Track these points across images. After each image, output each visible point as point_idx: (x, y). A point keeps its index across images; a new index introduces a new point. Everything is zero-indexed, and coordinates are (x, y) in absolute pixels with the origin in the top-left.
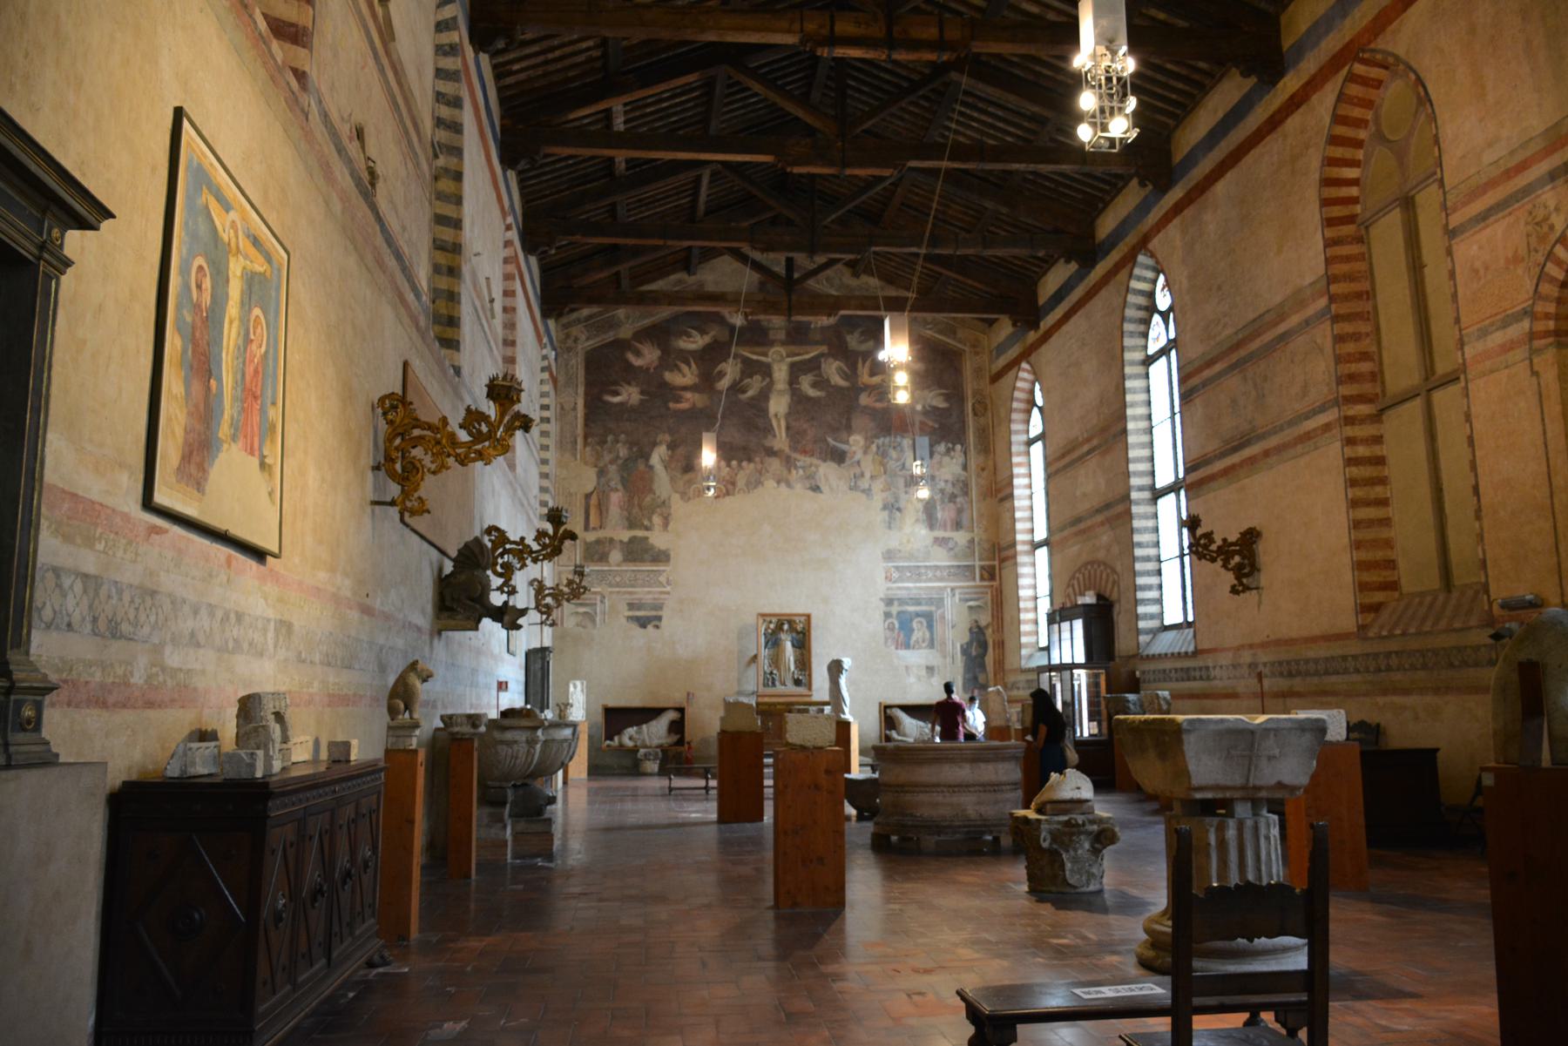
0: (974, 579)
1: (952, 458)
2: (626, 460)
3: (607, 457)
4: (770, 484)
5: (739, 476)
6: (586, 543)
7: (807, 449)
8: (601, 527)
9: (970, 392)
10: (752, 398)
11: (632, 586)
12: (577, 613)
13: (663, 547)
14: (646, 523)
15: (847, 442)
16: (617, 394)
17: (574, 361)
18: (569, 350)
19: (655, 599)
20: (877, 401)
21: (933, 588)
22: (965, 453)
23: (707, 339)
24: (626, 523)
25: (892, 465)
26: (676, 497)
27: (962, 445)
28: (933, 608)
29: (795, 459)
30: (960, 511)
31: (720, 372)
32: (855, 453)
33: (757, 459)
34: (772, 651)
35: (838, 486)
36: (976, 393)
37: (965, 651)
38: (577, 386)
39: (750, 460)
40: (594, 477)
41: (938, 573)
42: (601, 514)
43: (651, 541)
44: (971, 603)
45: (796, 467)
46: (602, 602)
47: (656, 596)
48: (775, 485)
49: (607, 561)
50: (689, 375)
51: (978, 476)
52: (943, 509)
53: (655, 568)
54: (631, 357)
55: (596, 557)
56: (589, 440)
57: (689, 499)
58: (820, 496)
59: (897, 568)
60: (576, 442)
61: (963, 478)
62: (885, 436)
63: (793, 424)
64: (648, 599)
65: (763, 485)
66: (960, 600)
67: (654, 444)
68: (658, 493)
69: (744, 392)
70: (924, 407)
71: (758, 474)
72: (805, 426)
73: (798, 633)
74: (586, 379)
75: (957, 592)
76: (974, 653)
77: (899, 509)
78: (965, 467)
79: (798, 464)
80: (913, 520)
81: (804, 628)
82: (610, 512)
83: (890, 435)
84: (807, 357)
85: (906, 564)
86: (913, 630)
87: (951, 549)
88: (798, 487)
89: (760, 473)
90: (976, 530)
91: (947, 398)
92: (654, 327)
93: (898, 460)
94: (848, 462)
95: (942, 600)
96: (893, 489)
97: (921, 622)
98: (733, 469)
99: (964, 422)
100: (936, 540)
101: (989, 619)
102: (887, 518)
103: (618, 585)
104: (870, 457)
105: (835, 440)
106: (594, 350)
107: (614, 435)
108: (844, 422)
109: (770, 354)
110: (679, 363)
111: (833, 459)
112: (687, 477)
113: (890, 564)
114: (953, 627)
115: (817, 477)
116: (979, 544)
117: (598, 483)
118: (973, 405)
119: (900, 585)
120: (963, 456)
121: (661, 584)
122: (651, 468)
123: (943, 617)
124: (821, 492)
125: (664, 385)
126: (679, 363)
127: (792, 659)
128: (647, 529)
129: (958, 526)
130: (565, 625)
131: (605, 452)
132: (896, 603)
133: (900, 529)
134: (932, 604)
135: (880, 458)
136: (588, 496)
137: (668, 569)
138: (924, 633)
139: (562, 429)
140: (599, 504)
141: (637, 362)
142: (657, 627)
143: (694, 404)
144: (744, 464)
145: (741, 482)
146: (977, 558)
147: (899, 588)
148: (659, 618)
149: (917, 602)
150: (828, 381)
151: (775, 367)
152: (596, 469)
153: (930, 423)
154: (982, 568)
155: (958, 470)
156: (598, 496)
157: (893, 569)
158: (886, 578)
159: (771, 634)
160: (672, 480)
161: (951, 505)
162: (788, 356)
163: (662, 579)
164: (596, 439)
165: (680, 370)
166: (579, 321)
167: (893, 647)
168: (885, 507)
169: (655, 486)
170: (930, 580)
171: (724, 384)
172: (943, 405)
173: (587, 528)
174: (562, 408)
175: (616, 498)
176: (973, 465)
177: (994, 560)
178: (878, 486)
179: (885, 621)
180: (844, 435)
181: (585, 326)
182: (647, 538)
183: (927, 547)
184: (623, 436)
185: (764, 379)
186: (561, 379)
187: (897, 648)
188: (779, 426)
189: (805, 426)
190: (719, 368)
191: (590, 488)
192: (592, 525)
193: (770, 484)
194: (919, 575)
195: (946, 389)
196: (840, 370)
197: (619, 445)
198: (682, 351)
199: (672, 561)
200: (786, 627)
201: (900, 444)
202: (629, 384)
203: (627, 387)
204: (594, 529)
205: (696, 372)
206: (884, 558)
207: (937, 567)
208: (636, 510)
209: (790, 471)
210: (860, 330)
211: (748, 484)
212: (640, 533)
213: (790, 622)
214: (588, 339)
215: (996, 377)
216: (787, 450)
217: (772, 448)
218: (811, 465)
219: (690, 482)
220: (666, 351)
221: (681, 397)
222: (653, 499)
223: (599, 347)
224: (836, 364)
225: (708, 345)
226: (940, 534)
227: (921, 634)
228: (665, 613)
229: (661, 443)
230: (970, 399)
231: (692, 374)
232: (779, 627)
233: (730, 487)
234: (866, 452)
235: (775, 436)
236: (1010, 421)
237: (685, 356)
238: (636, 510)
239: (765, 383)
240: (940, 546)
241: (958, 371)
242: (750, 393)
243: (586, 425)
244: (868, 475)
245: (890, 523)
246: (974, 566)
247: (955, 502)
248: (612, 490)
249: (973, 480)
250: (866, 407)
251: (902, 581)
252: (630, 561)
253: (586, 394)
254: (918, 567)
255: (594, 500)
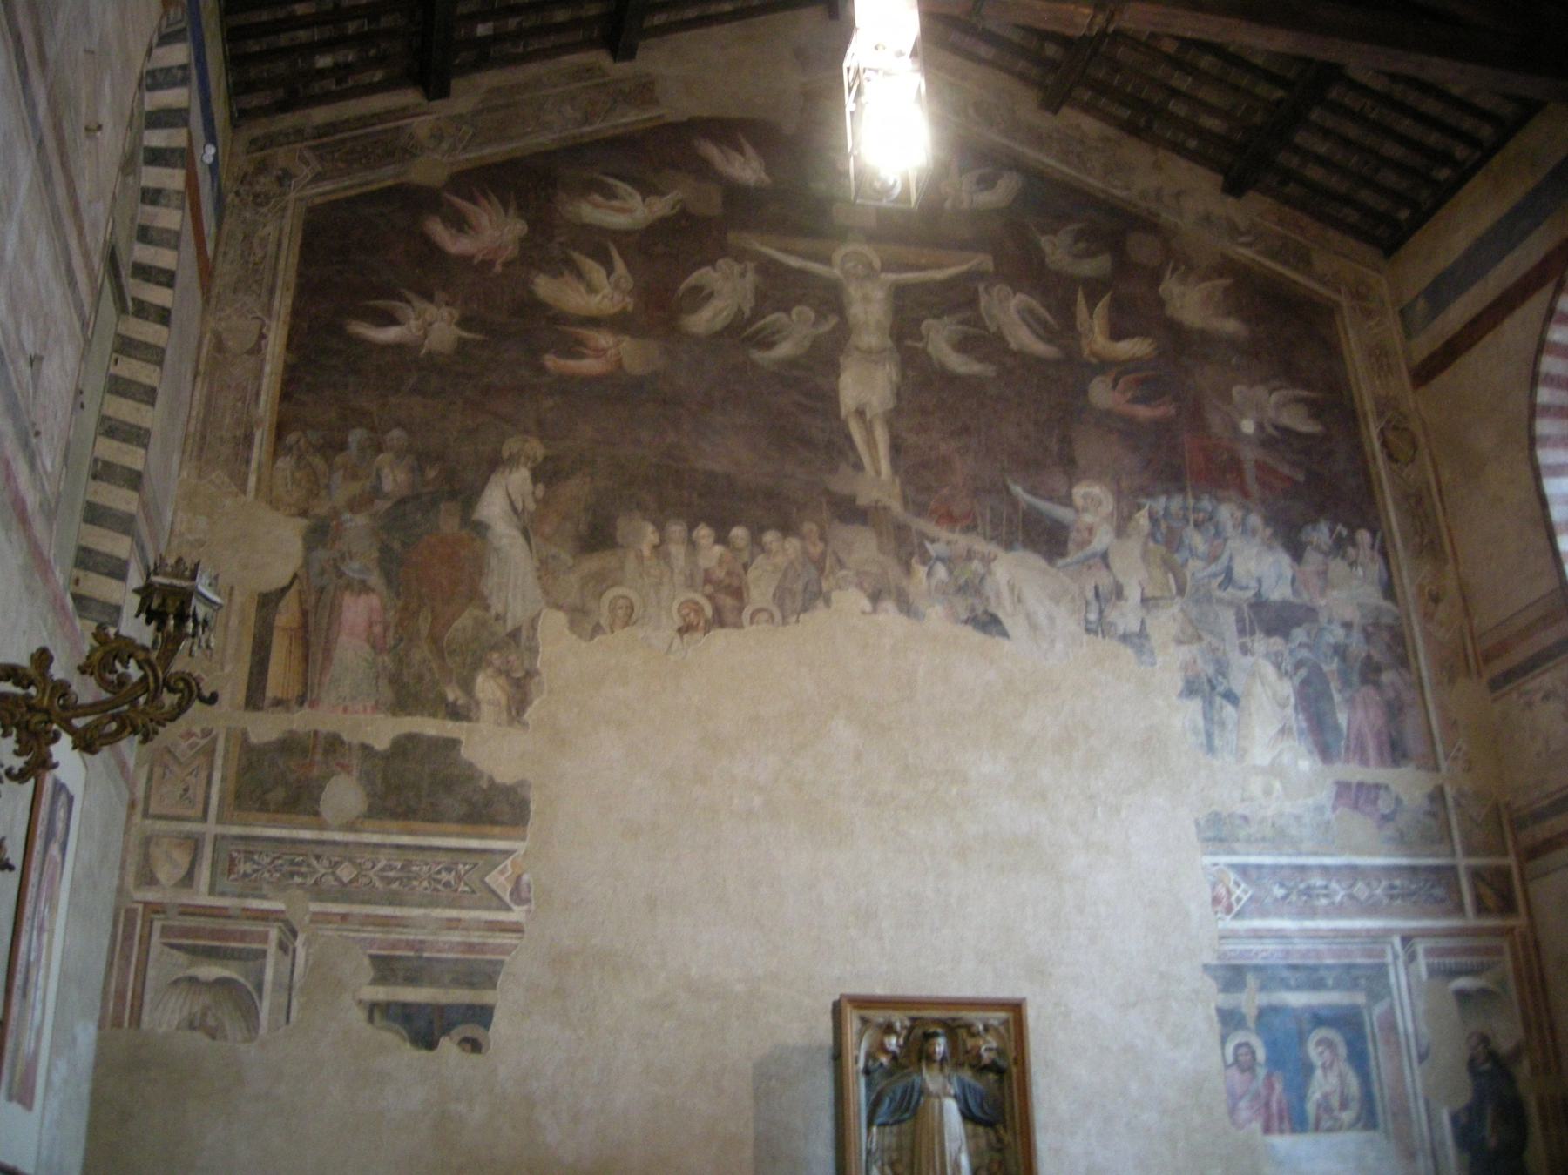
0: (1459, 909)
1: (1353, 564)
2: (402, 501)
3: (343, 491)
4: (852, 600)
5: (752, 574)
6: (246, 747)
7: (957, 511)
8: (301, 701)
9: (1369, 405)
10: (792, 363)
11: (394, 900)
12: (193, 980)
13: (505, 774)
14: (452, 693)
15: (1067, 501)
16: (390, 319)
17: (270, 230)
18: (260, 200)
19: (470, 947)
20: (1135, 400)
21: (1350, 934)
22: (1384, 554)
23: (661, 207)
24: (387, 693)
25: (1196, 568)
26: (554, 624)
27: (1374, 533)
28: (1360, 999)
29: (923, 535)
30: (1394, 710)
31: (697, 290)
32: (1090, 530)
33: (809, 527)
34: (890, 1137)
35: (1051, 619)
36: (1383, 406)
37: (1466, 1134)
38: (272, 291)
39: (787, 529)
40: (296, 547)
41: (1360, 889)
42: (306, 658)
43: (466, 753)
44: (1462, 983)
45: (925, 559)
46: (283, 947)
47: (475, 938)
48: (866, 604)
49: (317, 814)
50: (607, 290)
51: (1428, 616)
52: (1350, 702)
53: (474, 843)
54: (439, 231)
55: (279, 794)
56: (291, 438)
57: (597, 629)
58: (1006, 645)
59: (1243, 870)
60: (248, 439)
61: (1387, 620)
62: (1168, 493)
63: (911, 439)
64: (447, 944)
65: (828, 602)
66: (1433, 972)
67: (495, 463)
68: (497, 607)
69: (770, 345)
70: (1260, 426)
71: (813, 572)
72: (943, 448)
73: (980, 1068)
74: (300, 275)
75: (1420, 947)
76: (1492, 1142)
77: (1231, 697)
78: (1389, 591)
79: (932, 549)
80: (1273, 729)
81: (1000, 1052)
82: (337, 654)
83: (1182, 490)
84: (939, 275)
85: (1267, 860)
86: (1307, 1069)
87: (1386, 818)
88: (936, 614)
89: (821, 570)
90: (1444, 765)
91: (1316, 410)
92: (512, 165)
93: (1213, 558)
94: (1074, 556)
95: (1380, 971)
96: (1207, 638)
97: (1327, 1043)
98: (736, 550)
99: (1369, 481)
100: (1343, 788)
101: (1519, 1033)
102: (1201, 723)
103: (345, 893)
104: (1134, 546)
105: (1033, 491)
106: (334, 205)
107: (373, 429)
108: (1054, 447)
109: (837, 257)
110: (576, 255)
111: (1031, 543)
112: (592, 563)
113: (1224, 859)
114: (1422, 1058)
115: (988, 590)
116: (1458, 804)
117: (306, 564)
118: (1382, 432)
119: (1257, 923)
120: (1376, 553)
121: (494, 899)
122: (480, 529)
123: (1390, 1026)
124: (1005, 634)
125: (532, 308)
126: (576, 255)
127: (964, 1160)
128: (455, 713)
129: (1395, 751)
130: (145, 1025)
131: (338, 476)
132: (1251, 980)
133: (1241, 754)
134: (1354, 985)
135: (1162, 549)
136: (268, 602)
137: (520, 846)
138: (1341, 1076)
139: (208, 403)
140: (304, 626)
141: (455, 244)
142: (474, 1045)
143: (619, 363)
144: (770, 537)
145: (760, 591)
146: (1458, 848)
147: (1257, 935)
148: (483, 1015)
149: (1312, 977)
150: (1000, 337)
151: (853, 292)
152: (303, 523)
153: (1285, 470)
154: (1476, 875)
155: (1373, 596)
156: (301, 602)
157: (1233, 876)
158: (1216, 900)
159: (889, 1073)
160: (545, 570)
161: (1369, 690)
162: (886, 267)
163: (499, 880)
164: (314, 436)
165: (580, 275)
166: (299, 132)
167: (1257, 1126)
168: (1191, 689)
169: (490, 584)
170: (1338, 911)
171: (703, 321)
172: (1305, 425)
173: (254, 698)
174: (219, 346)
175: (357, 611)
176: (1407, 583)
177: (1505, 854)
178: (1166, 623)
179: (1224, 1040)
180: (1058, 481)
181: (312, 148)
182: (453, 744)
183: (1319, 809)
184: (396, 434)
185: (821, 316)
186: (226, 270)
187: (1267, 1130)
188: (871, 444)
189: (943, 448)
190: (693, 279)
191: (279, 572)
192: (271, 692)
193: (852, 600)
194: (1308, 892)
195: (1307, 385)
196: (1027, 315)
197: (384, 458)
198: (588, 228)
199: (534, 819)
200: (940, 1046)
201: (1211, 519)
202: (428, 296)
203: (419, 304)
204: (278, 703)
205: (628, 282)
206: (1208, 840)
207: (1354, 872)
208: (421, 653)
209: (908, 570)
210: (1075, 226)
211: (780, 596)
212: (430, 727)
213: (952, 1029)
214: (318, 178)
215: (1424, 373)
216: (896, 506)
217: (853, 499)
218: (970, 556)
219: (601, 581)
220: (542, 226)
221: (580, 342)
222: (481, 624)
223: (349, 200)
224: (1018, 300)
225: (664, 220)
226: (1355, 772)
227: (1333, 1080)
228: (505, 999)
229: (513, 461)
230: (1371, 418)
231: (616, 287)
232: (917, 1050)
233: (728, 602)
234: (1122, 528)
235: (858, 466)
236: (1532, 442)
237: (599, 244)
238: (421, 653)
239: (825, 327)
240: (1356, 807)
241: (1332, 350)
242: (784, 350)
243: (285, 396)
244: (1133, 594)
245: (1209, 735)
246: (1453, 869)
247: (1377, 685)
248: (349, 586)
249: (1417, 629)
250: (1108, 413)
251: (1264, 914)
252: (394, 815)
253: (295, 313)
254: (1303, 869)
255: (287, 615)
